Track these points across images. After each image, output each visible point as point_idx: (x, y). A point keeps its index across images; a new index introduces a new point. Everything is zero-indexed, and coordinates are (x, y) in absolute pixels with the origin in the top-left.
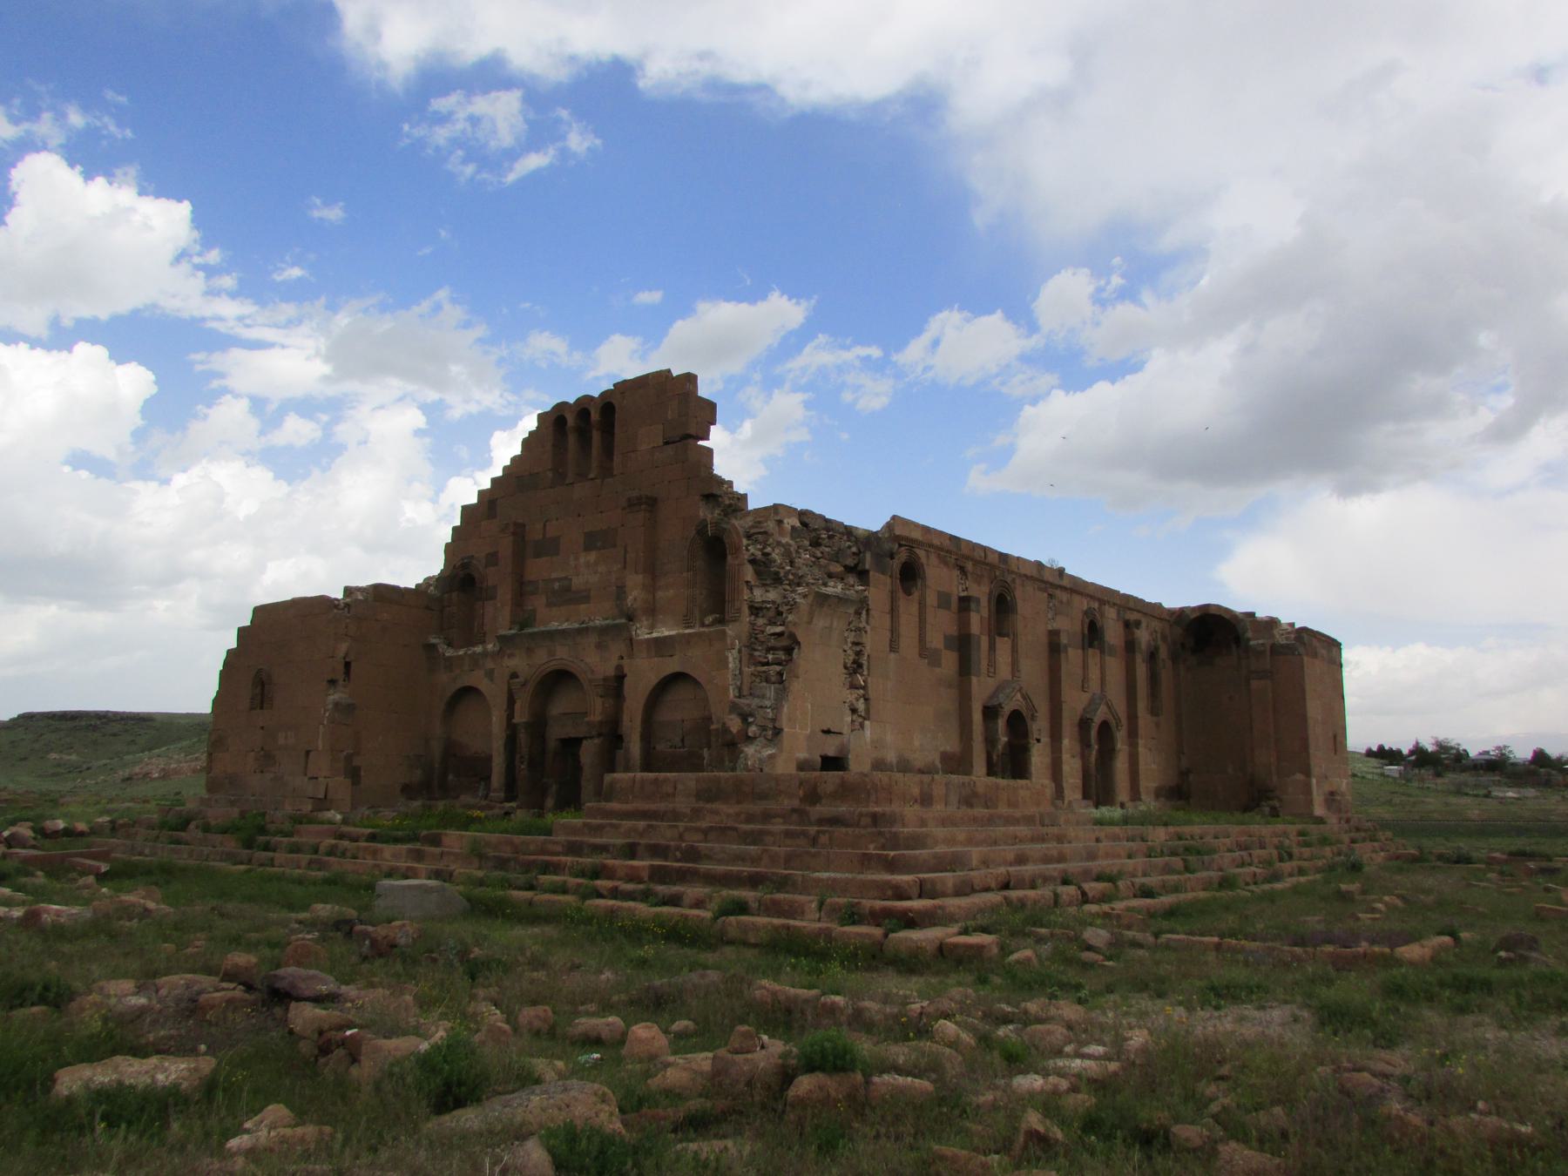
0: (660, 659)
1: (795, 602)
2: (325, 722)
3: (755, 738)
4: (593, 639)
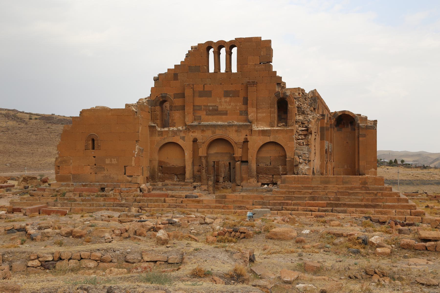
0: (264, 137)
1: (310, 121)
2: (135, 156)
3: (302, 163)
4: (234, 129)
